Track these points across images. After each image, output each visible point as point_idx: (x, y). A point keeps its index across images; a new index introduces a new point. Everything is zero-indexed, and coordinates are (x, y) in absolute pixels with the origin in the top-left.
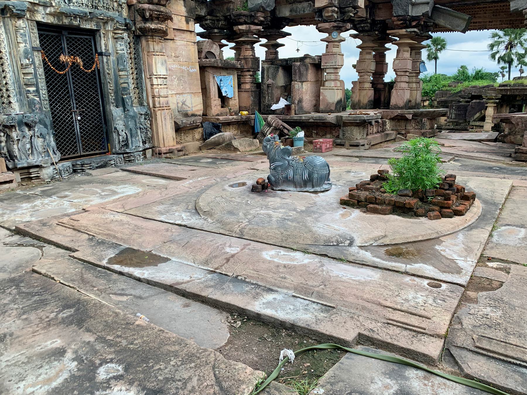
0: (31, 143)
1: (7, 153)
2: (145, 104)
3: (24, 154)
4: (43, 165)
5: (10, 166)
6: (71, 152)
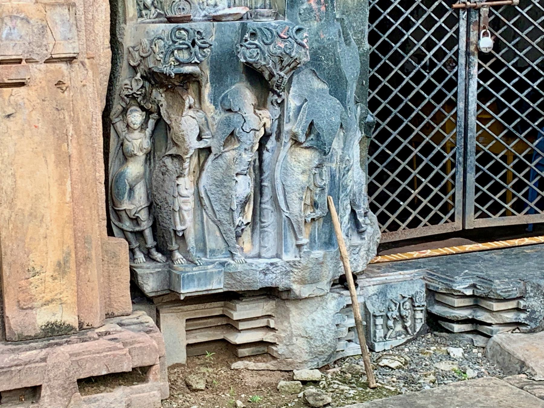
0: (259, 169)
1: (143, 215)
3: (218, 224)
4: (295, 287)
5: (150, 286)
6: (425, 212)
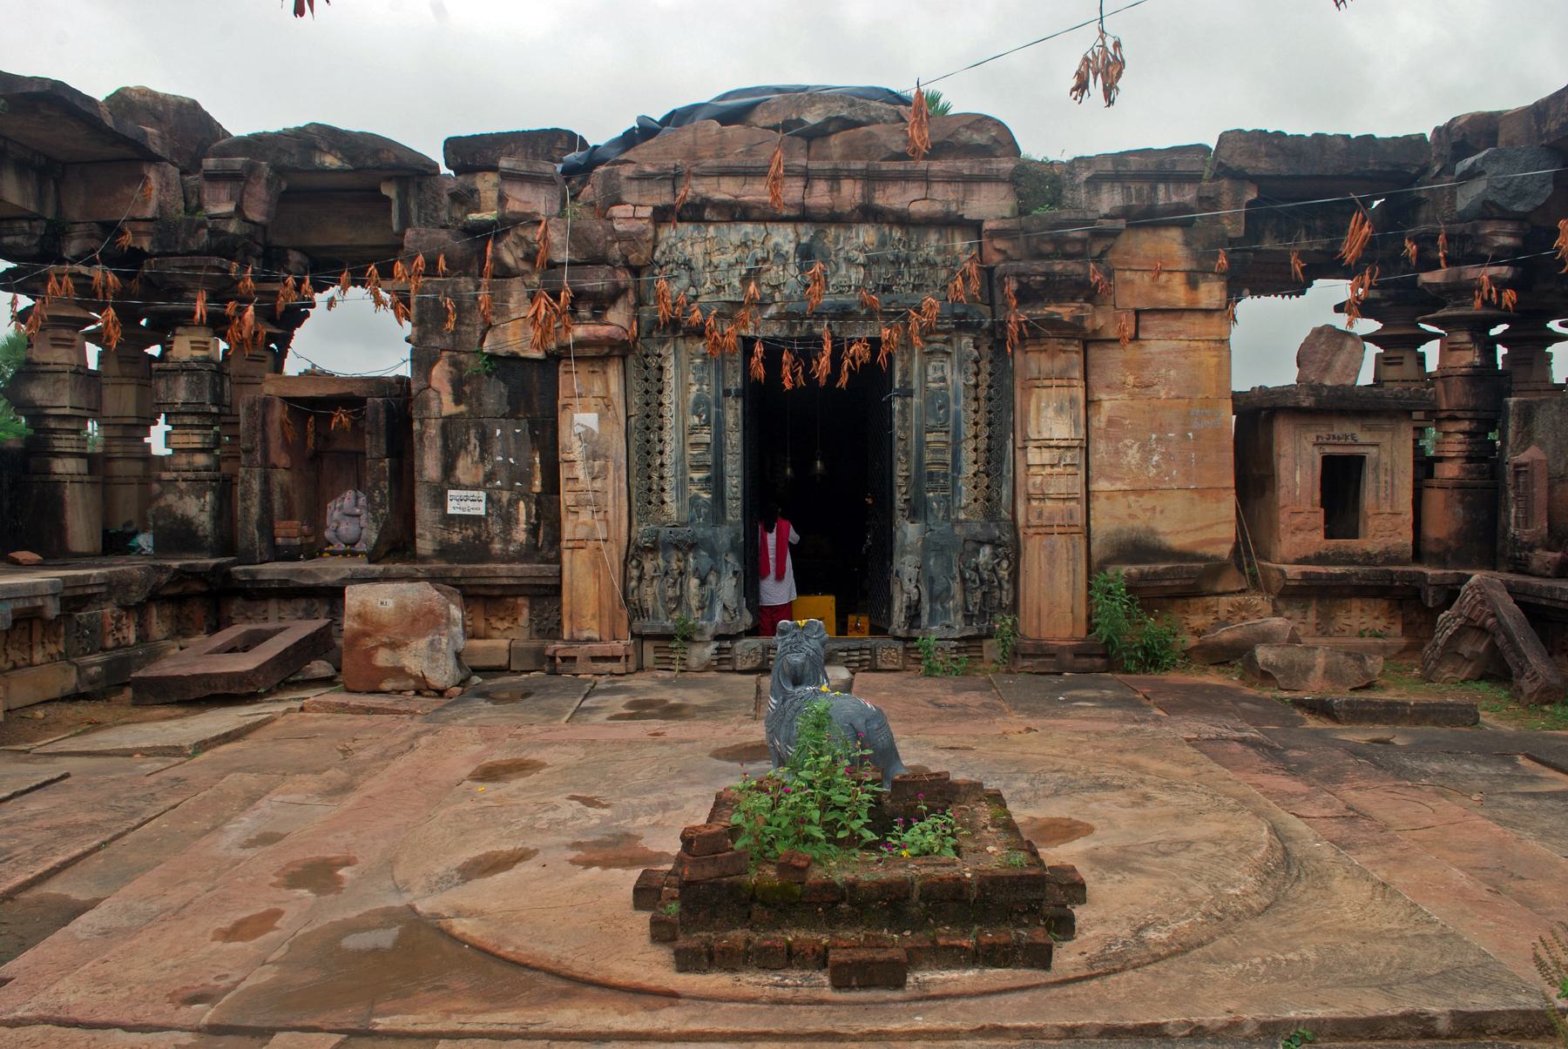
2: (1005, 514)
